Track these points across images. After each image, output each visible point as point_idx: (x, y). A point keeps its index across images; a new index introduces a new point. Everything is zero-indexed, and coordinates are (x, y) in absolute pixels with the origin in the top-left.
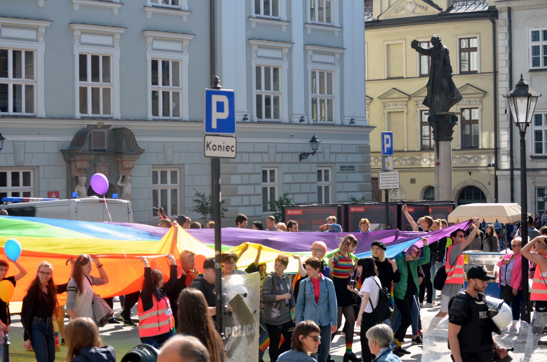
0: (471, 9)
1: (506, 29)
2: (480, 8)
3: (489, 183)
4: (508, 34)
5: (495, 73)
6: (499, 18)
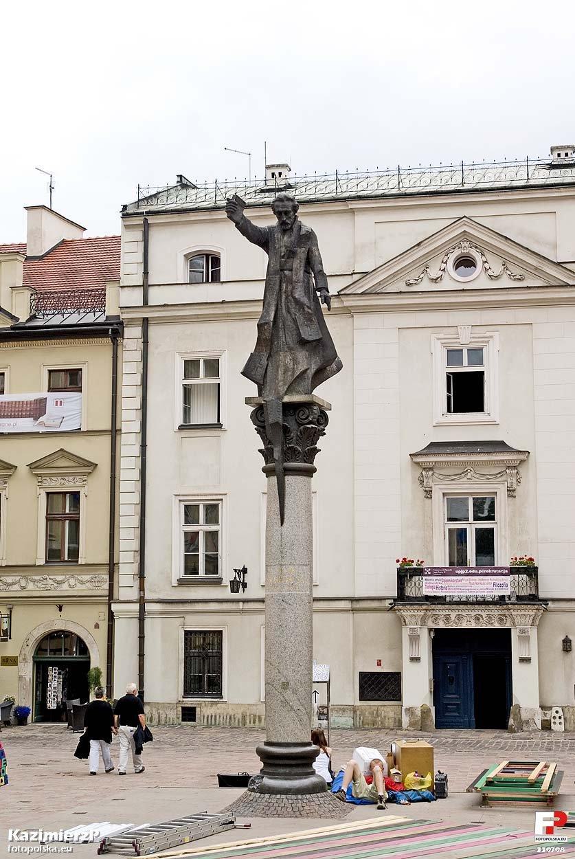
0: (73, 319)
1: (138, 356)
2: (90, 318)
3: (97, 626)
4: (141, 365)
5: (114, 432)
6: (125, 336)
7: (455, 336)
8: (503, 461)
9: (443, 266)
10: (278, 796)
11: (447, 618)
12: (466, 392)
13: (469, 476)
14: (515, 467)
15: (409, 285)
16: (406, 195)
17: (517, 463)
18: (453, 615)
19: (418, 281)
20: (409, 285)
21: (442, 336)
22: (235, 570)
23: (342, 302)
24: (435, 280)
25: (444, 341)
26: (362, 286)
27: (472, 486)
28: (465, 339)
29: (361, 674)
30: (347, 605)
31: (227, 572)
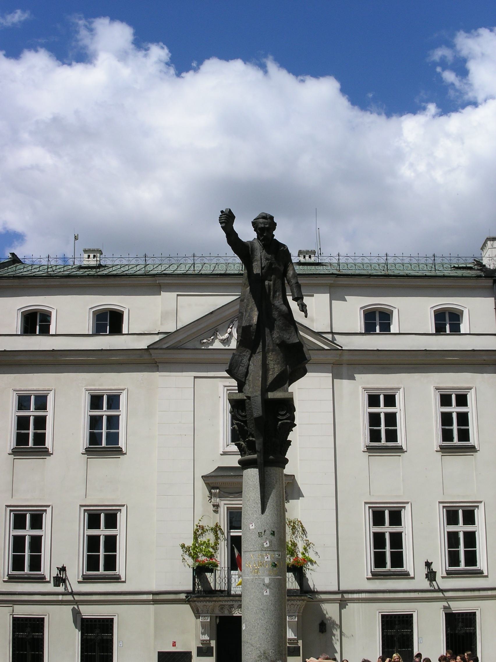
21: (228, 384)
22: (58, 568)
24: (223, 342)
26: (165, 344)
29: (159, 653)
30: (150, 597)
31: (48, 569)
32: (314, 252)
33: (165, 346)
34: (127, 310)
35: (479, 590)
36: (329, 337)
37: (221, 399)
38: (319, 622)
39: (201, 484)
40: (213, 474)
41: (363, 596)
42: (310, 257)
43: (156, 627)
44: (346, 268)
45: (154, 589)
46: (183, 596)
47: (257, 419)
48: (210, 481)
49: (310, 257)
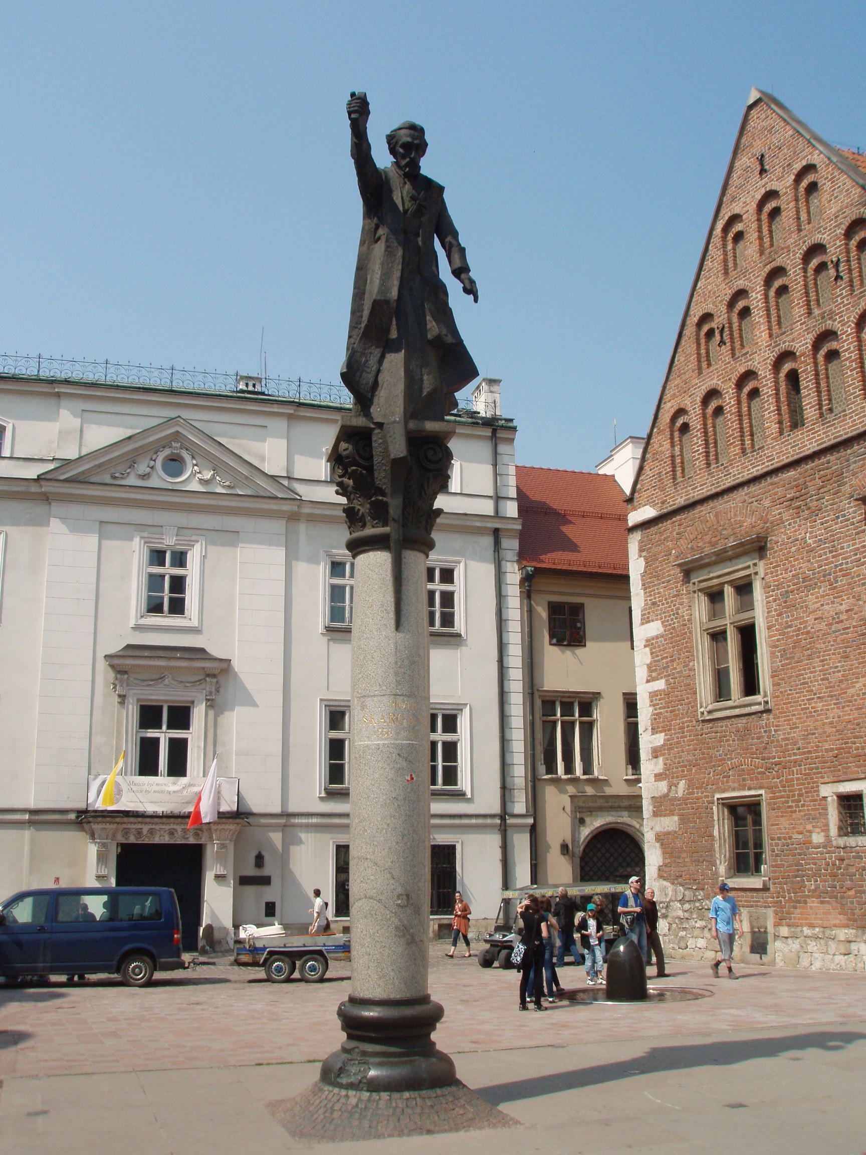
7: (157, 536)
8: (204, 668)
9: (152, 463)
10: (407, 1094)
11: (139, 832)
12: (167, 596)
13: (166, 682)
14: (214, 676)
15: (114, 478)
16: (118, 387)
17: (216, 672)
18: (145, 829)
19: (124, 476)
20: (114, 478)
23: (41, 486)
24: (144, 477)
25: (147, 540)
26: (63, 474)
27: (165, 695)
28: (169, 541)
30: (27, 817)
32: (260, 380)
33: (62, 477)
34: (11, 425)
35: (460, 816)
36: (285, 483)
37: (136, 555)
38: (255, 853)
39: (102, 665)
40: (120, 653)
41: (315, 820)
42: (254, 386)
43: (32, 857)
44: (308, 397)
45: (32, 805)
46: (72, 816)
47: (396, 462)
48: (116, 661)
49: (254, 386)
